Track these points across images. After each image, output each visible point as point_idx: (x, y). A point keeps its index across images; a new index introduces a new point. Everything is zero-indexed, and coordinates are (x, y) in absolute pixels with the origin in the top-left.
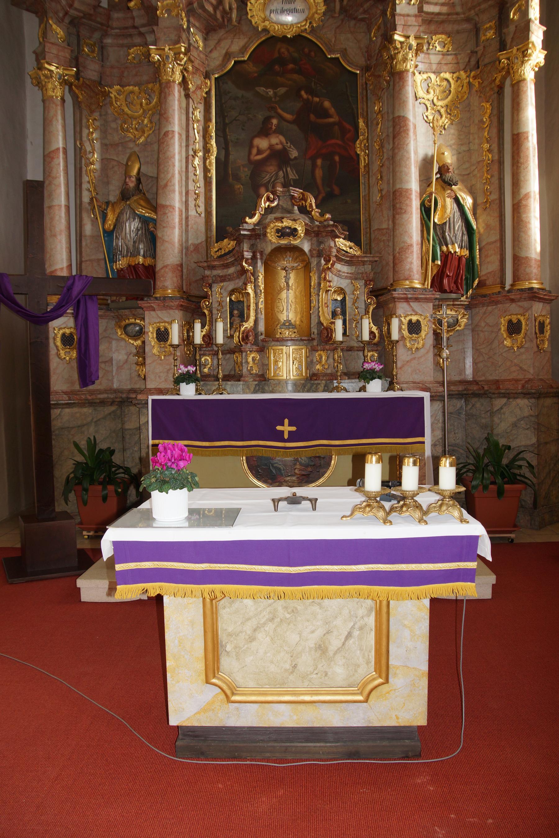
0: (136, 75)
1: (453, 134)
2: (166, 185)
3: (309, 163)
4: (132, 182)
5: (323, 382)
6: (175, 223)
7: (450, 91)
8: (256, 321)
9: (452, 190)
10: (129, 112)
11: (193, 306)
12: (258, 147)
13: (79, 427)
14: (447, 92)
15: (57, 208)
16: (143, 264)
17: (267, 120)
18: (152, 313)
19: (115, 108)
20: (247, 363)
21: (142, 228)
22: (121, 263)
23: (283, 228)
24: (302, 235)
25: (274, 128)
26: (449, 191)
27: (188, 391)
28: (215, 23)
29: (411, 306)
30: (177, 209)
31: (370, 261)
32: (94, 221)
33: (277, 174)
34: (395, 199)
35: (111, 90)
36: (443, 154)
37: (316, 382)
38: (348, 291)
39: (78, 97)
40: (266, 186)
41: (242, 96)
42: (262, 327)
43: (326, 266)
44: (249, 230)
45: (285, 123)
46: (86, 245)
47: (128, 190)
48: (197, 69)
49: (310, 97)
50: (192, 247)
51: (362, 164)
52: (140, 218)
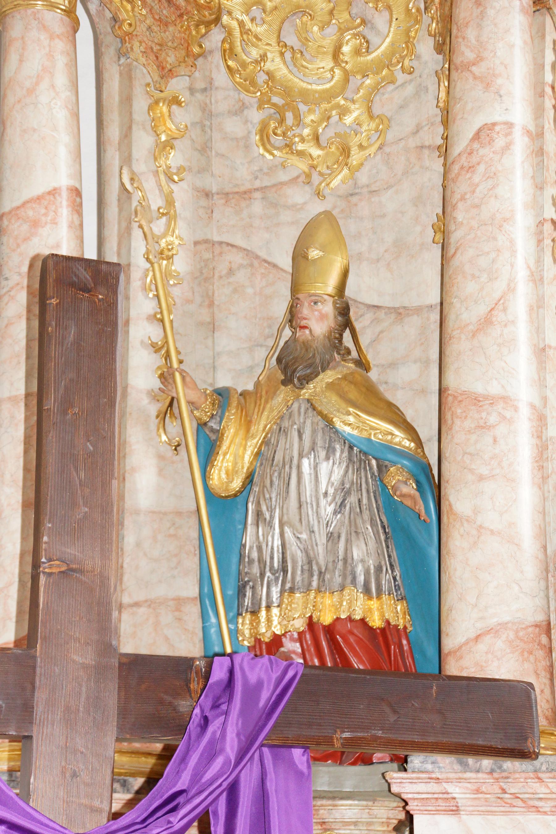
19: (244, 65)
22: (282, 617)
46: (138, 544)
52: (351, 448)
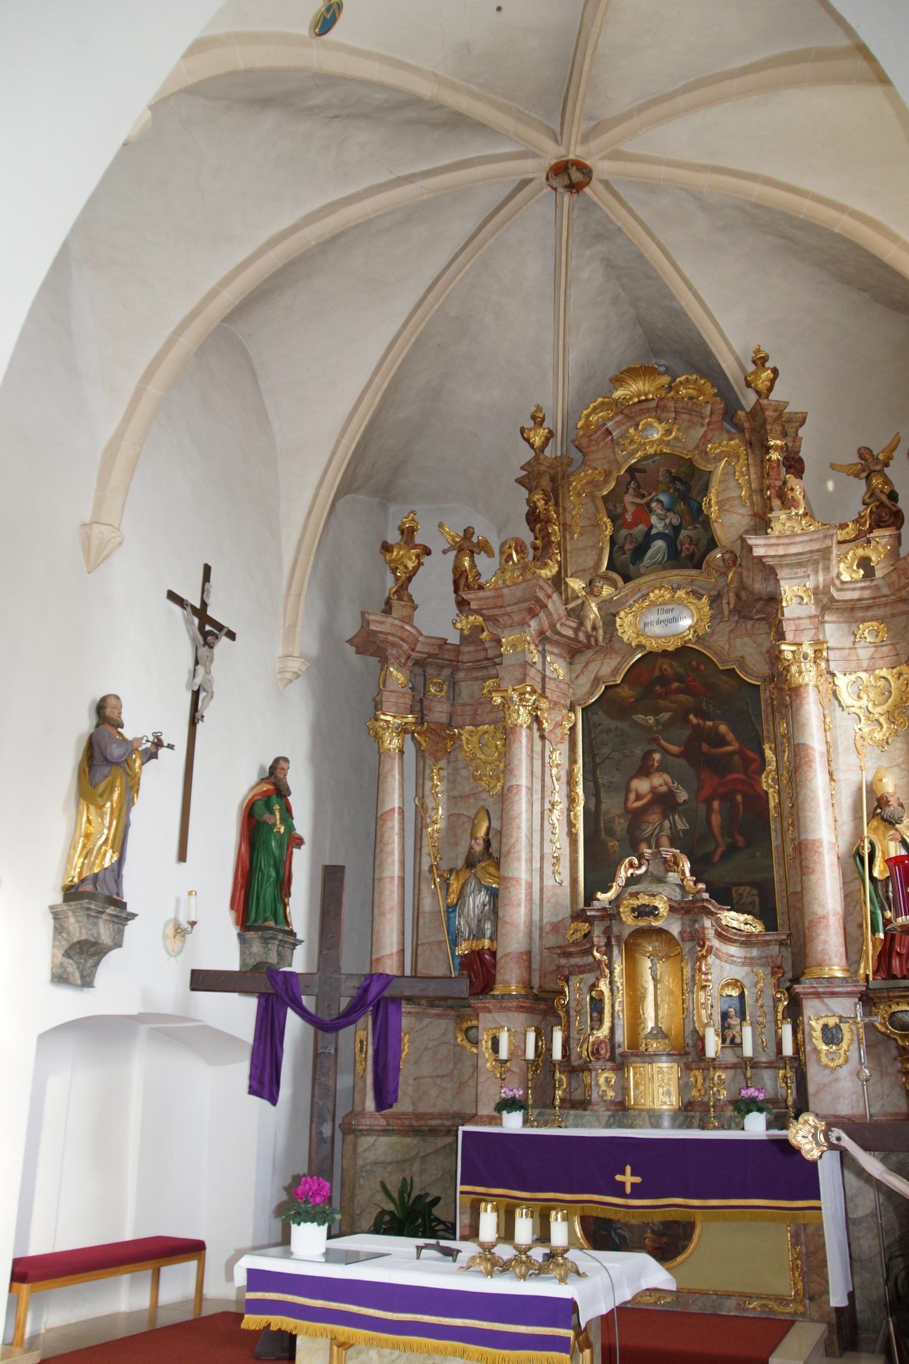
0: (491, 711)
1: (901, 749)
2: (509, 852)
3: (703, 807)
4: (478, 844)
5: (698, 1114)
6: (520, 900)
7: (890, 692)
8: (612, 1030)
9: (897, 830)
10: (483, 757)
11: (543, 1005)
12: (636, 791)
13: (398, 1162)
15: (387, 880)
16: (489, 949)
17: (648, 755)
18: (488, 1015)
19: (466, 752)
20: (597, 1085)
21: (489, 902)
23: (639, 907)
24: (665, 914)
25: (656, 764)
26: (893, 832)
28: (579, 645)
29: (826, 1004)
30: (523, 883)
31: (776, 940)
32: (434, 894)
33: (661, 824)
35: (461, 732)
36: (881, 780)
37: (690, 1114)
38: (746, 982)
39: (421, 745)
40: (648, 841)
41: (616, 728)
42: (621, 1037)
43: (700, 953)
44: (598, 910)
45: (670, 758)
46: (424, 924)
47: (473, 854)
48: (556, 703)
49: (701, 721)
50: (548, 926)
51: (772, 804)
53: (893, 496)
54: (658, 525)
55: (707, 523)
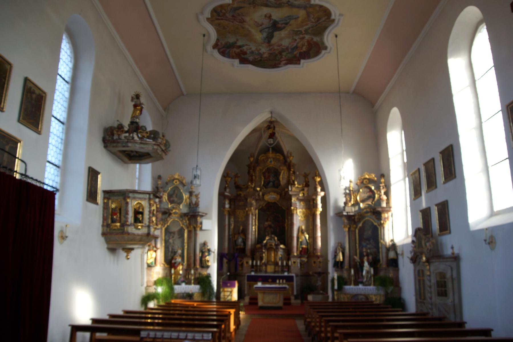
14: (303, 213)
27: (253, 274)
34: (292, 237)
53: (308, 182)
54: (271, 179)
55: (279, 181)
